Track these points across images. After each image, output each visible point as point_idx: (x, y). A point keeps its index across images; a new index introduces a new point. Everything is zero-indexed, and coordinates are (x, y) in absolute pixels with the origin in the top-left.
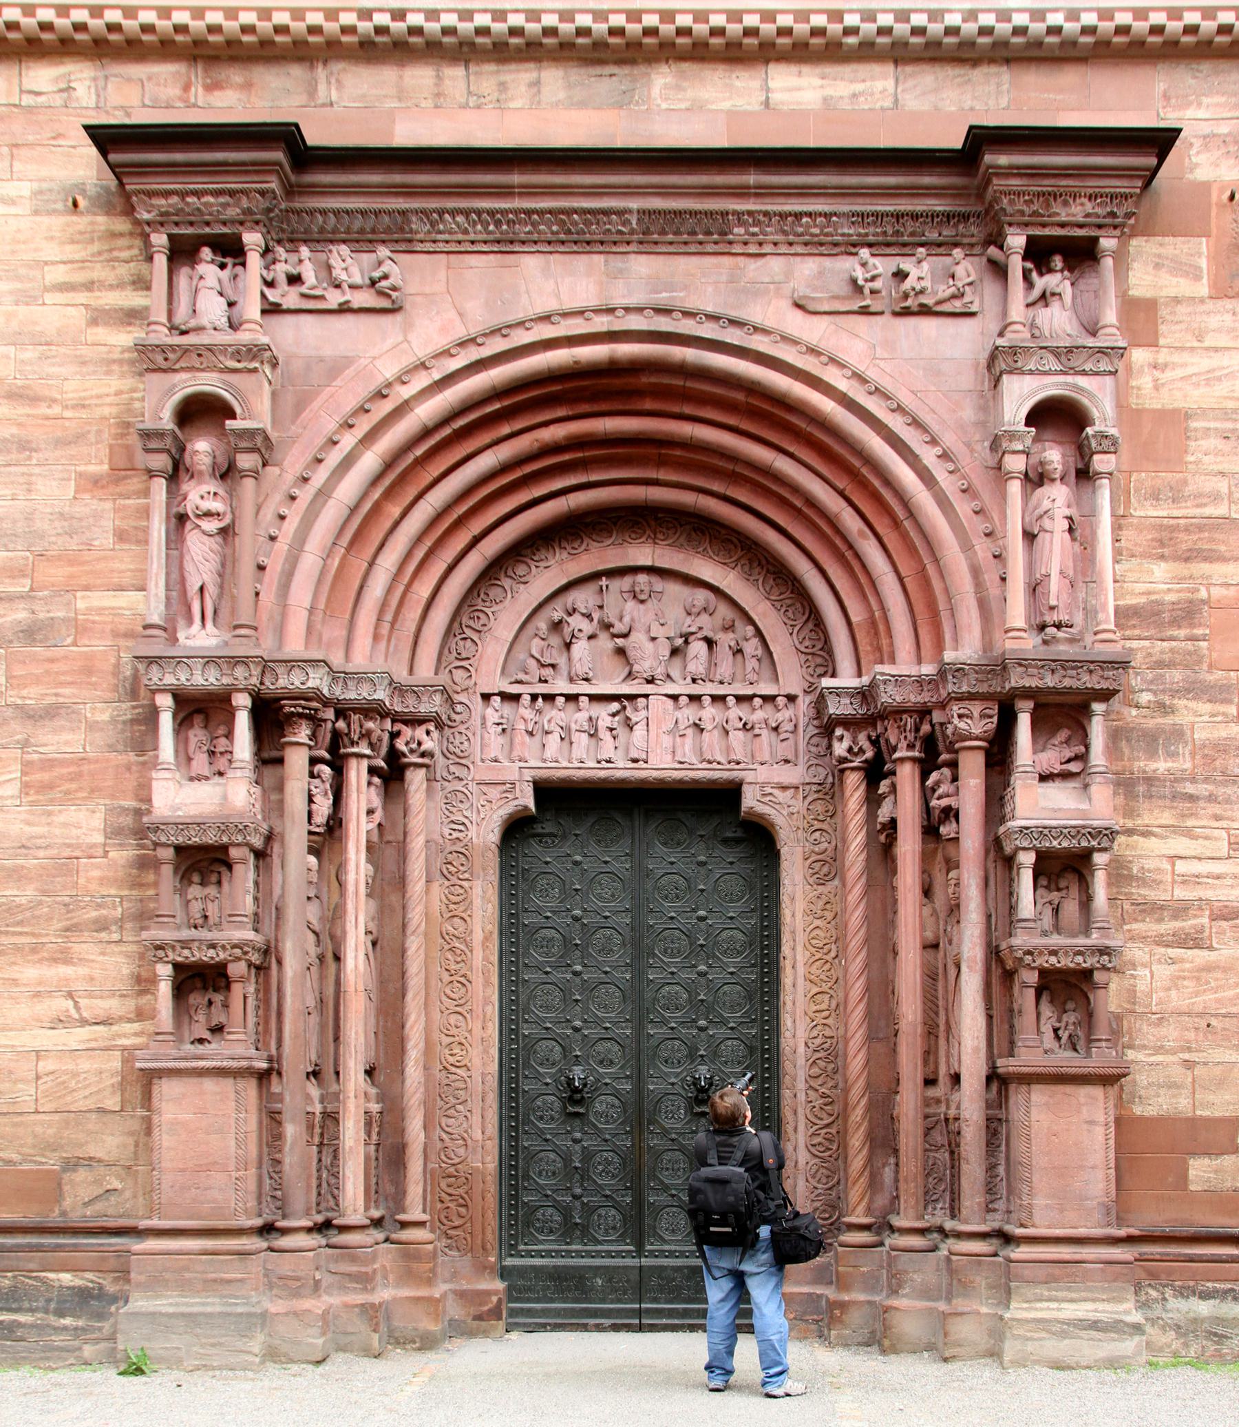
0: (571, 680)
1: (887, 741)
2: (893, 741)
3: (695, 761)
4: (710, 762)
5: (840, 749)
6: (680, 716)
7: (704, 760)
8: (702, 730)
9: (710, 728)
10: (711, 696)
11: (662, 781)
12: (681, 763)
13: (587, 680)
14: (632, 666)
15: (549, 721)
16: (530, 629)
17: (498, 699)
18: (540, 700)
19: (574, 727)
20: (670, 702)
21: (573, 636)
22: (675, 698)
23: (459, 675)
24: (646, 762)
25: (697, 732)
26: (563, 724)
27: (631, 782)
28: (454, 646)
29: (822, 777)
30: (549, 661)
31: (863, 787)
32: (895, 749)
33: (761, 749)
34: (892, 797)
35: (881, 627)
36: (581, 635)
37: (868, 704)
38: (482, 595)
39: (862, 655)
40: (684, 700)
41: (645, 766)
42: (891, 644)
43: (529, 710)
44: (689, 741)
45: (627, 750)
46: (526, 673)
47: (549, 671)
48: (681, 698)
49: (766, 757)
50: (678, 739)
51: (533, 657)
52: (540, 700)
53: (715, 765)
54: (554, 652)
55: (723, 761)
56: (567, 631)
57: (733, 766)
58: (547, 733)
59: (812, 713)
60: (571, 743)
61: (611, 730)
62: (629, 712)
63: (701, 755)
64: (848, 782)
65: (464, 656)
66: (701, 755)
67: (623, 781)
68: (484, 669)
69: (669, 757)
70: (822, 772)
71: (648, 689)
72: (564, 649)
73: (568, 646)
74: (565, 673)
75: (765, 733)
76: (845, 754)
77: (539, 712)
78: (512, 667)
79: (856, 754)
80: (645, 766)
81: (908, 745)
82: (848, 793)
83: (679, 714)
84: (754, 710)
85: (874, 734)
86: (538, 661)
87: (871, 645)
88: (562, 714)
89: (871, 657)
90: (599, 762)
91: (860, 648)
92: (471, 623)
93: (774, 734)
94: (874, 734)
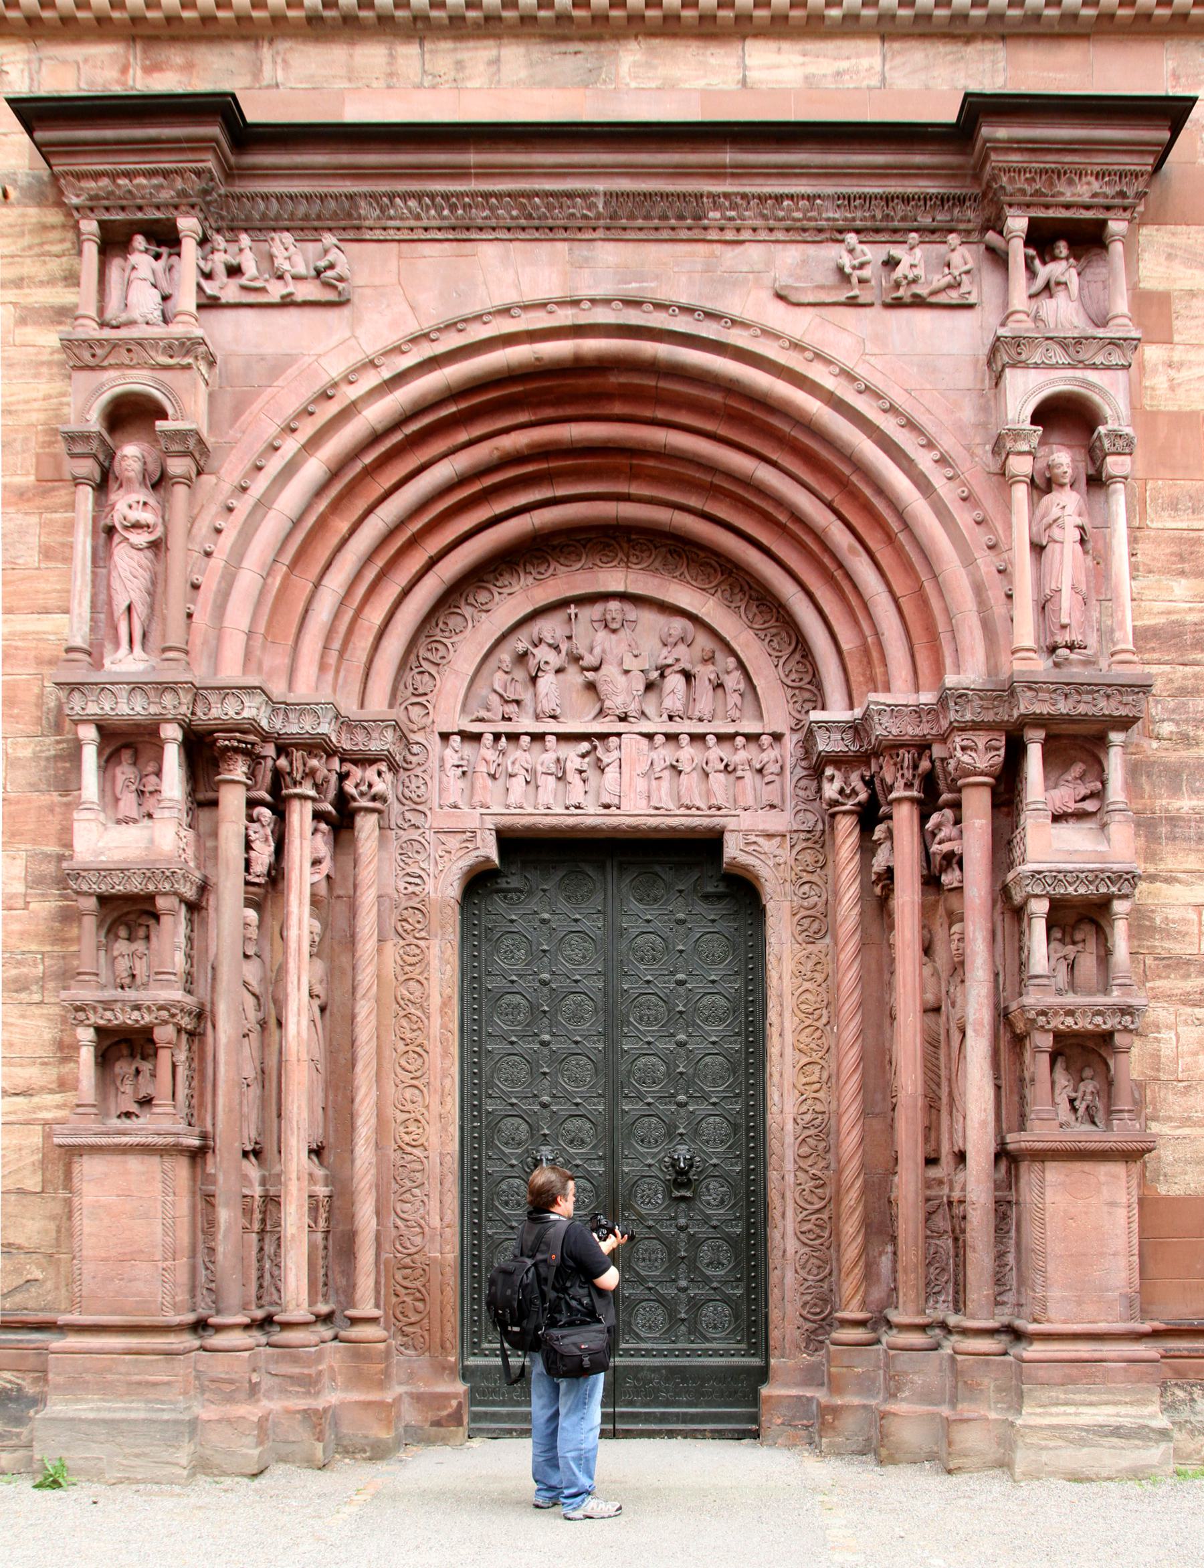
0: (537, 717)
1: (882, 780)
2: (889, 780)
3: (672, 807)
4: (688, 808)
5: (830, 790)
6: (655, 757)
7: (682, 806)
8: (680, 772)
9: (688, 769)
10: (689, 734)
11: (636, 829)
12: (657, 808)
13: (554, 717)
14: (602, 701)
15: (513, 763)
16: (493, 662)
17: (458, 738)
18: (503, 739)
19: (540, 769)
20: (645, 741)
21: (539, 669)
22: (650, 736)
23: (416, 712)
24: (619, 808)
25: (675, 774)
26: (529, 767)
27: (602, 830)
28: (410, 681)
29: (811, 823)
30: (513, 697)
31: (857, 832)
32: (891, 789)
33: (744, 793)
34: (888, 844)
35: (875, 655)
36: (547, 668)
37: (861, 740)
38: (441, 625)
39: (854, 686)
40: (659, 739)
41: (618, 812)
42: (886, 673)
43: (491, 751)
44: (665, 784)
45: (598, 795)
46: (488, 710)
47: (511, 709)
48: (656, 737)
49: (750, 801)
50: (654, 783)
51: (495, 691)
52: (503, 739)
53: (694, 811)
54: (519, 687)
55: (703, 806)
56: (532, 663)
57: (713, 811)
58: (511, 776)
59: (800, 752)
60: (537, 787)
61: (581, 772)
62: (600, 752)
63: (679, 799)
64: (840, 827)
65: (421, 691)
66: (679, 799)
67: (594, 829)
68: (442, 705)
69: (644, 803)
70: (811, 819)
71: (620, 727)
72: (529, 684)
73: (534, 680)
74: (531, 711)
75: (748, 775)
76: (836, 796)
77: (503, 752)
78: (473, 703)
79: (848, 797)
80: (618, 812)
81: (906, 784)
82: (839, 840)
83: (654, 755)
84: (737, 749)
85: (867, 774)
86: (501, 696)
87: (864, 675)
88: (527, 755)
89: (864, 689)
90: (567, 808)
91: (852, 678)
92: (429, 655)
93: (758, 777)
94: (867, 774)
